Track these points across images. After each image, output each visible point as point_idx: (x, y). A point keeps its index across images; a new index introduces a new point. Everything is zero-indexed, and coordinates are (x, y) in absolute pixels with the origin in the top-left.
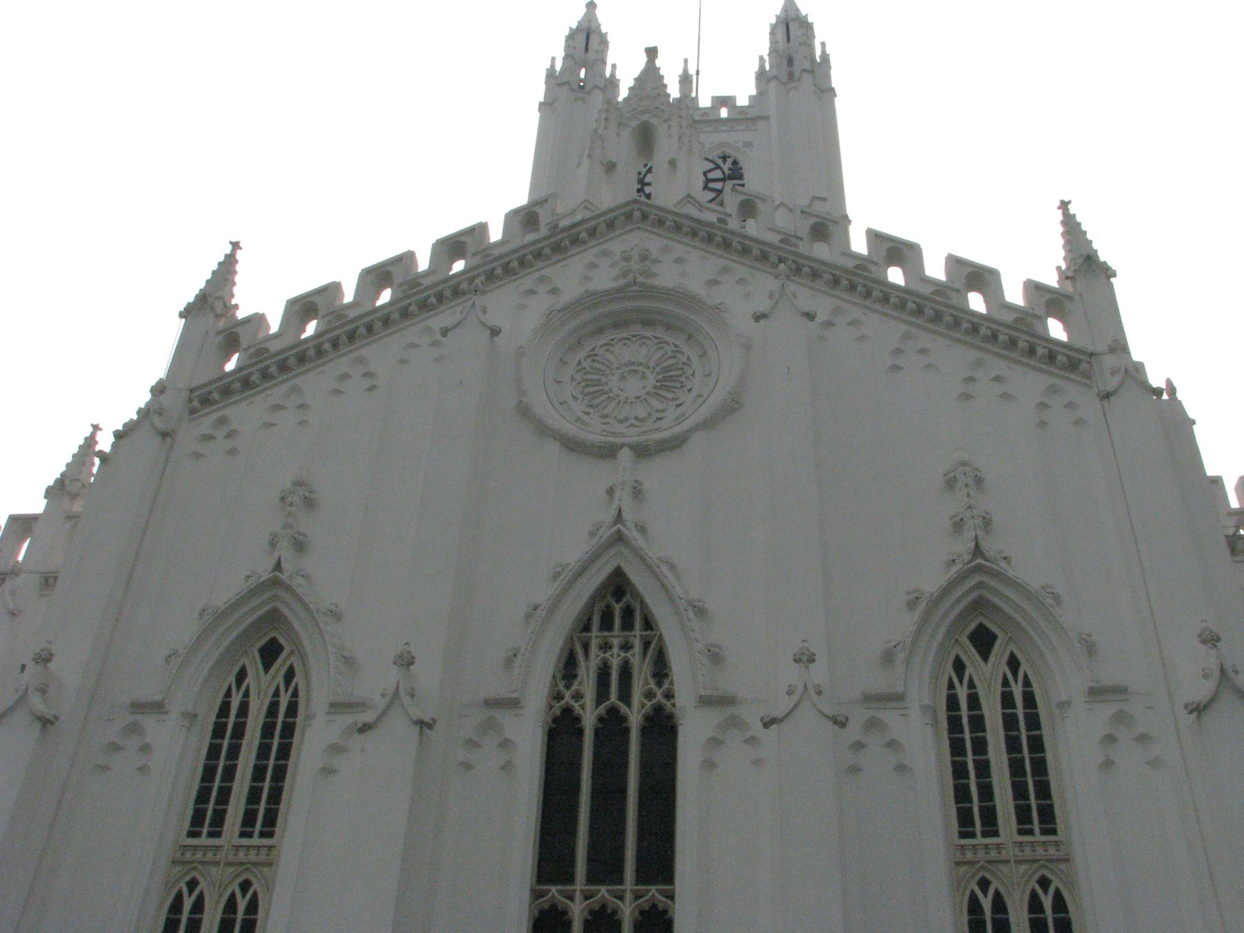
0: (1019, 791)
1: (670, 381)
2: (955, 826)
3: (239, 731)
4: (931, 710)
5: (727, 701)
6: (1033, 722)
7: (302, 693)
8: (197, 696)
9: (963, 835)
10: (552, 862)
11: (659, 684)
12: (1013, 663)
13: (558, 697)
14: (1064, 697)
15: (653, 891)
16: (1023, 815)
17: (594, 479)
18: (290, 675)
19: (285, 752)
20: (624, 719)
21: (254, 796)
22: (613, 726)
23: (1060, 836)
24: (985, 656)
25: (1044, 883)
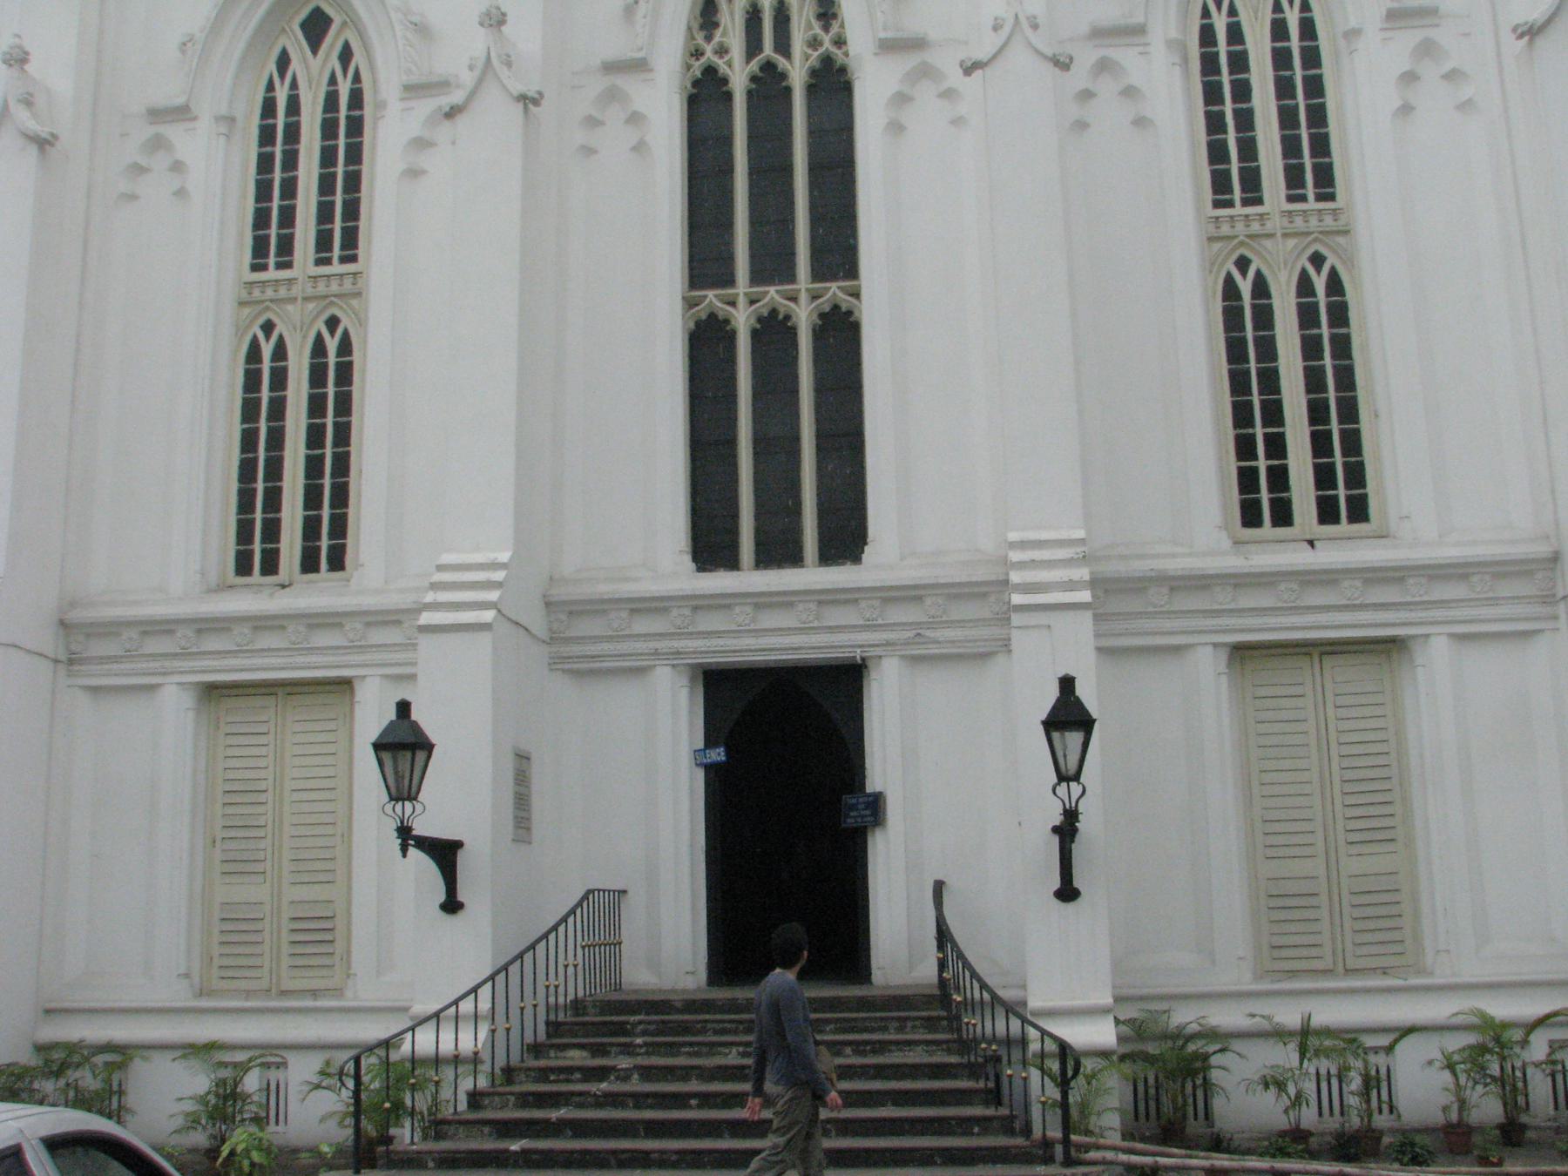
0: (1290, 147)
2: (1208, 195)
3: (293, 133)
4: (1180, 46)
5: (916, 44)
6: (1312, 58)
7: (365, 75)
8: (228, 94)
9: (1217, 204)
10: (706, 264)
11: (826, 28)
13: (697, 53)
14: (1353, 23)
15: (834, 290)
16: (1294, 177)
18: (346, 55)
19: (355, 154)
20: (783, 76)
21: (325, 213)
23: (1340, 202)
25: (1317, 260)
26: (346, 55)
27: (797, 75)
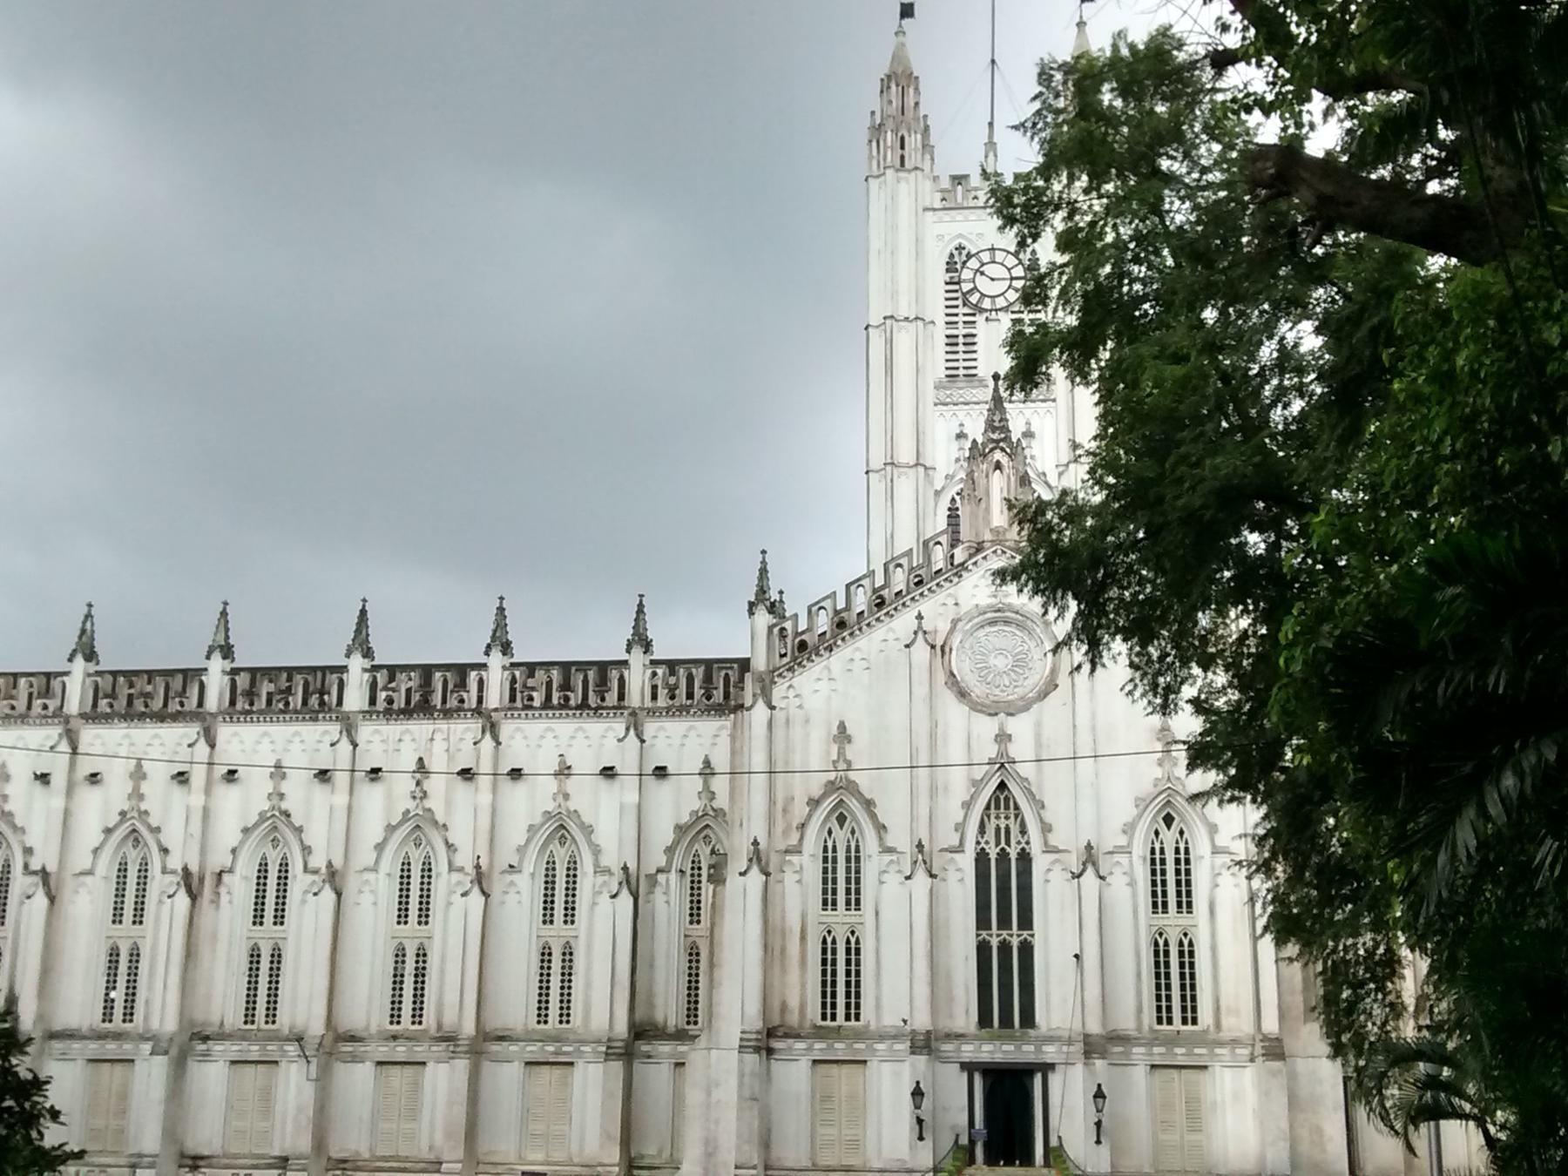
1: (1020, 663)
3: (835, 860)
4: (1145, 859)
5: (1057, 851)
6: (1187, 862)
10: (982, 922)
12: (1181, 833)
13: (978, 843)
15: (1025, 933)
16: (1179, 905)
17: (987, 727)
18: (853, 832)
21: (848, 891)
22: (1003, 856)
24: (1169, 827)
26: (853, 832)
27: (1013, 856)
